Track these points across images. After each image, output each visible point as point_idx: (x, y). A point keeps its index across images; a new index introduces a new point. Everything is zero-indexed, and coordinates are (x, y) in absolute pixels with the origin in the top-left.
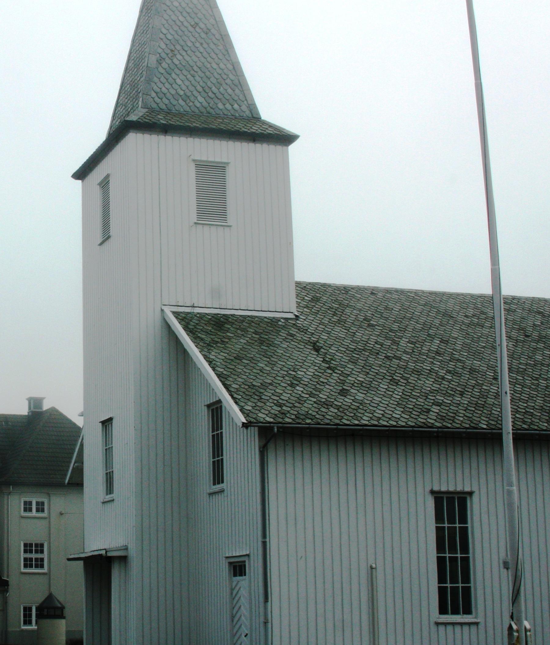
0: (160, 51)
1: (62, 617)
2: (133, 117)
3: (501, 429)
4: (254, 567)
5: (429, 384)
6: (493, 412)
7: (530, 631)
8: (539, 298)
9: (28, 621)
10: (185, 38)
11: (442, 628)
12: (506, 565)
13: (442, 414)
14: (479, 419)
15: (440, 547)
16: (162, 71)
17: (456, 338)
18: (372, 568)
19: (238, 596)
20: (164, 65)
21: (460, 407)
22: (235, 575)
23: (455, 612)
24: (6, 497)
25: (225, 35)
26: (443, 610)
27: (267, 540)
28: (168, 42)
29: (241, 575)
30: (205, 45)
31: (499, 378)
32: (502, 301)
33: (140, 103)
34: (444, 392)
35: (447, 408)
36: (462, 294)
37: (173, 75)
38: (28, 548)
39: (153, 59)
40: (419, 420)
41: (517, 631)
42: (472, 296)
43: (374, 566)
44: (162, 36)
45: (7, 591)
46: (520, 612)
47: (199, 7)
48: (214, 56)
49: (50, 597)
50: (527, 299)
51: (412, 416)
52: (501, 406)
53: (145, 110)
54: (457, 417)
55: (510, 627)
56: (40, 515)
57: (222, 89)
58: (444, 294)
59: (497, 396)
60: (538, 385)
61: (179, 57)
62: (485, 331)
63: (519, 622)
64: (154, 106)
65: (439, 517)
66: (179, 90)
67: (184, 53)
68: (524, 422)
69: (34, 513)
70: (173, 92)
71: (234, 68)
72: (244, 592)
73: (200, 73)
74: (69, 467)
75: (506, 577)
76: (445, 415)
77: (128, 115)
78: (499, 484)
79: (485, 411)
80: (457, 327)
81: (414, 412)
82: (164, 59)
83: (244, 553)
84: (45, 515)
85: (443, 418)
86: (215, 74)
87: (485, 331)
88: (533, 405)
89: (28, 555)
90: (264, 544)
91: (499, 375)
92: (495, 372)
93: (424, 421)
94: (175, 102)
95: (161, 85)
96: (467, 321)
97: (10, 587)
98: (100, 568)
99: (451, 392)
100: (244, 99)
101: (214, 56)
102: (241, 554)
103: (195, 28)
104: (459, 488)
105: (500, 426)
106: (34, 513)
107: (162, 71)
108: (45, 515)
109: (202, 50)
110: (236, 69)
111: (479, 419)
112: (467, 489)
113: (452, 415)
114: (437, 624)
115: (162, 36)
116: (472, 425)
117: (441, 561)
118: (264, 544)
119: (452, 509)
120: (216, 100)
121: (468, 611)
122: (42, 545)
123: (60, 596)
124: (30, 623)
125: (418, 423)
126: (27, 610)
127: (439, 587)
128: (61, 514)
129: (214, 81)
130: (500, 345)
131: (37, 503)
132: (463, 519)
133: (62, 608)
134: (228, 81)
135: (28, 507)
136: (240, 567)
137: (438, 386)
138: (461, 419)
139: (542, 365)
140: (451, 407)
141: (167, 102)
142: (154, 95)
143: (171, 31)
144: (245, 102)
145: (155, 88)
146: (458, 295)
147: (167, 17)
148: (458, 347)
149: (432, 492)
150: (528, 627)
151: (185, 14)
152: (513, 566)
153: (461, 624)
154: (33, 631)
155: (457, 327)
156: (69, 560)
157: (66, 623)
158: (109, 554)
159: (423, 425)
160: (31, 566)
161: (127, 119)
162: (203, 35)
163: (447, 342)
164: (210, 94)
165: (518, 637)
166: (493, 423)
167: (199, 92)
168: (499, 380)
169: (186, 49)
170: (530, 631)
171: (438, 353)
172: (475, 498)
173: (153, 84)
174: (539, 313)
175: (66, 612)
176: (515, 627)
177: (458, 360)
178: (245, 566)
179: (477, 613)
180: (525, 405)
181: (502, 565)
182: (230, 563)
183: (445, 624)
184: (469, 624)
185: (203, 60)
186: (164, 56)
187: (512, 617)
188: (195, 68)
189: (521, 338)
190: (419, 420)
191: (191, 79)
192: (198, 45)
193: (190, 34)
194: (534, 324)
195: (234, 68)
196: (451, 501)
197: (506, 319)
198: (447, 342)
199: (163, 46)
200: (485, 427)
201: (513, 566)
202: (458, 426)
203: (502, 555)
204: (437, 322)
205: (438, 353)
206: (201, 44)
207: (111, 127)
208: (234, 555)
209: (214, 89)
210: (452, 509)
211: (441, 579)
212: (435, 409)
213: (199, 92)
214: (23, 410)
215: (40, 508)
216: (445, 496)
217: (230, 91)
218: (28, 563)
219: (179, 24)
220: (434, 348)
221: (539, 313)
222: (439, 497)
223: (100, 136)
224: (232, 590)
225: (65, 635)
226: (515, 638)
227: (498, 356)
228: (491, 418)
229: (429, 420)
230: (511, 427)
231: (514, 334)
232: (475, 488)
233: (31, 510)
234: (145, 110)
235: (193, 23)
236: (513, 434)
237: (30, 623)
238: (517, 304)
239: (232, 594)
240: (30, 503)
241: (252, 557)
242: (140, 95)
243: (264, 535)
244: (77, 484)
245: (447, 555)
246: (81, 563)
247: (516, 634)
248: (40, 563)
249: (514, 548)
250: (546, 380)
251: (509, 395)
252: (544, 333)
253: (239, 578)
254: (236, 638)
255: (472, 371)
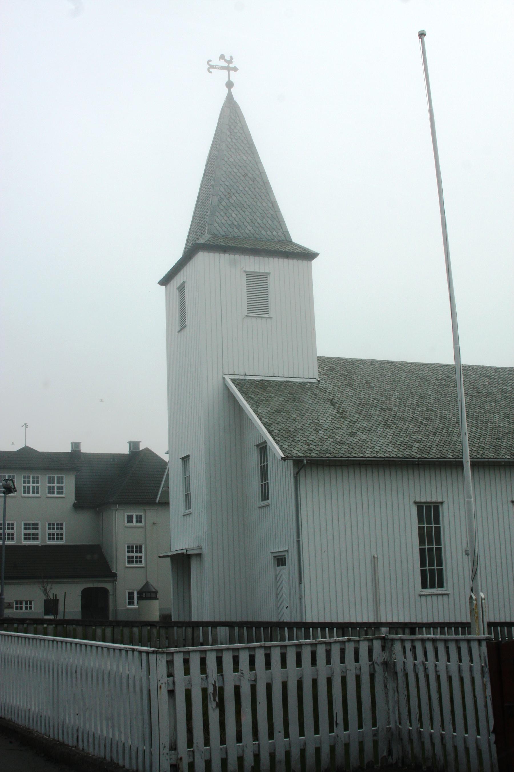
0: (220, 193)
1: (156, 598)
2: (201, 241)
3: (462, 458)
4: (291, 559)
5: (411, 427)
6: (457, 446)
7: (484, 599)
8: (487, 367)
9: (131, 602)
10: (238, 184)
11: (423, 598)
12: (467, 553)
13: (421, 448)
14: (447, 452)
15: (421, 541)
16: (222, 208)
17: (430, 395)
18: (374, 558)
19: (281, 580)
20: (224, 203)
21: (434, 444)
22: (278, 565)
23: (433, 586)
24: (114, 513)
25: (266, 182)
26: (424, 586)
27: (301, 539)
28: (226, 187)
29: (282, 565)
30: (252, 190)
31: (460, 422)
32: (462, 369)
33: (206, 231)
34: (423, 433)
35: (425, 444)
36: (434, 364)
37: (230, 211)
38: (130, 549)
39: (216, 199)
40: (406, 453)
41: (476, 600)
42: (441, 366)
43: (376, 556)
44: (222, 183)
45: (116, 581)
46: (477, 586)
47: (248, 162)
48: (259, 197)
49: (147, 584)
50: (478, 367)
51: (400, 450)
52: (461, 442)
53: (209, 236)
54: (431, 450)
55: (471, 597)
56: (139, 525)
57: (264, 220)
58: (421, 364)
59: (459, 435)
60: (487, 427)
61: (234, 198)
62: (450, 390)
63: (477, 594)
64: (216, 232)
65: (420, 520)
66: (234, 221)
67: (237, 195)
68: (478, 453)
69: (134, 524)
70: (230, 223)
71: (273, 206)
72: (285, 577)
73: (249, 209)
74: (159, 490)
75: (467, 562)
76: (423, 449)
77: (198, 239)
78: (461, 497)
79: (451, 446)
80: (431, 387)
81: (401, 447)
82: (223, 199)
83: (285, 550)
84: (142, 525)
85: (422, 451)
86: (260, 210)
87: (450, 390)
88: (484, 441)
89: (131, 555)
90: (298, 542)
91: (460, 420)
92: (458, 418)
93: (409, 453)
94: (231, 230)
95: (221, 218)
96: (437, 383)
97: (118, 578)
98: (182, 562)
99: (427, 433)
100: (280, 228)
101: (259, 197)
102: (282, 550)
103: (245, 177)
104: (434, 500)
105: (461, 456)
106: (134, 524)
107: (222, 208)
108: (142, 525)
109: (250, 193)
110: (274, 206)
111: (447, 452)
112: (440, 500)
113: (428, 449)
114: (421, 596)
115: (222, 183)
116: (442, 455)
117: (422, 552)
118: (298, 542)
119: (429, 514)
120: (261, 229)
121: (441, 586)
122: (140, 547)
123: (154, 584)
124: (133, 603)
125: (405, 455)
126: (131, 594)
127: (421, 570)
128: (154, 524)
129: (259, 215)
130: (461, 400)
131: (137, 517)
132: (437, 521)
133: (156, 592)
134: (269, 215)
135: (130, 519)
136: (282, 559)
137: (418, 429)
138: (435, 451)
139: (490, 413)
140: (428, 443)
141: (225, 230)
142: (216, 225)
143: (228, 179)
144: (281, 230)
145: (217, 220)
146: (431, 364)
147: (224, 169)
148: (432, 401)
149: (415, 503)
150: (483, 596)
151: (237, 167)
152: (472, 554)
153: (437, 595)
154: (135, 609)
155: (431, 387)
156: (160, 557)
157: (159, 603)
158: (189, 553)
159: (408, 456)
160: (133, 562)
161: (197, 242)
162: (251, 182)
163: (424, 398)
164: (256, 224)
165: (476, 604)
166: (456, 454)
167: (249, 223)
168: (460, 424)
169: (239, 192)
170: (484, 599)
171: (417, 405)
172: (445, 506)
173: (215, 217)
174: (487, 376)
175: (159, 595)
176: (474, 597)
177: (432, 410)
178: (285, 558)
179: (447, 586)
180: (478, 441)
181: (464, 554)
182: (275, 557)
183: (426, 595)
184: (443, 595)
185: (251, 200)
186: (223, 196)
187: (472, 590)
188: (245, 205)
189: (475, 394)
190: (406, 453)
191: (243, 213)
192: (247, 189)
193: (242, 182)
194: (484, 385)
195: (273, 206)
196: (428, 508)
197: (464, 381)
198: (424, 398)
199: (223, 191)
200: (451, 457)
201: (472, 554)
202: (432, 456)
203: (464, 546)
204: (416, 384)
205: (417, 405)
206: (250, 189)
207: (186, 248)
208: (277, 551)
209: (259, 220)
210: (429, 514)
211: (423, 563)
212: (416, 445)
213: (249, 223)
214: (125, 450)
215: (139, 520)
216: (424, 505)
217: (270, 222)
218: (131, 560)
219: (234, 174)
220: (415, 402)
221: (487, 376)
222: (420, 507)
223: (178, 254)
224: (276, 576)
225: (158, 611)
226: (475, 605)
227: (460, 407)
228: (455, 451)
229: (412, 453)
230: (469, 457)
231: (470, 391)
232: (445, 499)
233: (132, 522)
234: (209, 236)
235: (243, 174)
236: (471, 462)
237: (133, 603)
238: (471, 371)
239: (276, 579)
240: (132, 517)
241: (290, 553)
242: (207, 225)
243: (298, 537)
244: (165, 504)
245: (427, 547)
246: (169, 559)
247: (475, 602)
248: (139, 560)
249: (472, 540)
250: (492, 423)
251: (467, 434)
252: (490, 391)
253: (281, 567)
254: (279, 610)
255: (442, 417)
